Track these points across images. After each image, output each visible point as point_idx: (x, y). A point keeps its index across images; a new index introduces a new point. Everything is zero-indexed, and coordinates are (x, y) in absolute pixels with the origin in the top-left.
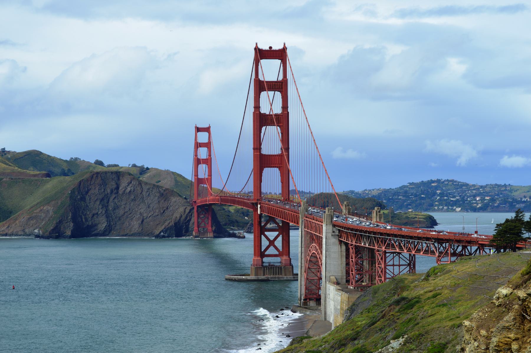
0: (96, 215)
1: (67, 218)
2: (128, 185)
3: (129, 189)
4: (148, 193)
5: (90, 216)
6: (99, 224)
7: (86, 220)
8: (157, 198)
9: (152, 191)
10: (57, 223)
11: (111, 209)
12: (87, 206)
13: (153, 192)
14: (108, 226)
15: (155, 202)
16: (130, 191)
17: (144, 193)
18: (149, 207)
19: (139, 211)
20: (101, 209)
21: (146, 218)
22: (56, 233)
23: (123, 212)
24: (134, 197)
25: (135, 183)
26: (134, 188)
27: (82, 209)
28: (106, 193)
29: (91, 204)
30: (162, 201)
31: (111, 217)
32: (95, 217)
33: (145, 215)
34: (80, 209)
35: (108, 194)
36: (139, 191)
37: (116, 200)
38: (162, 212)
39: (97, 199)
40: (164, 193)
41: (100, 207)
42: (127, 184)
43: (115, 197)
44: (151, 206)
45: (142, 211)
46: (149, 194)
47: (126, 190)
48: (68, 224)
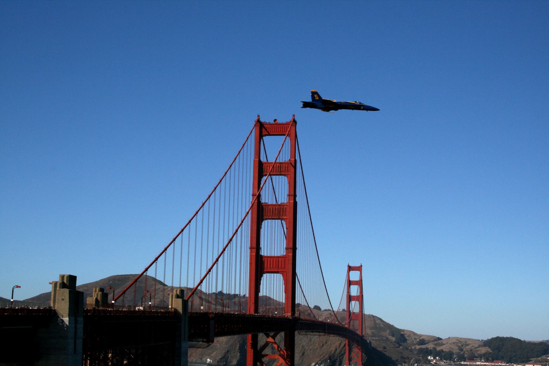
21: (308, 350)
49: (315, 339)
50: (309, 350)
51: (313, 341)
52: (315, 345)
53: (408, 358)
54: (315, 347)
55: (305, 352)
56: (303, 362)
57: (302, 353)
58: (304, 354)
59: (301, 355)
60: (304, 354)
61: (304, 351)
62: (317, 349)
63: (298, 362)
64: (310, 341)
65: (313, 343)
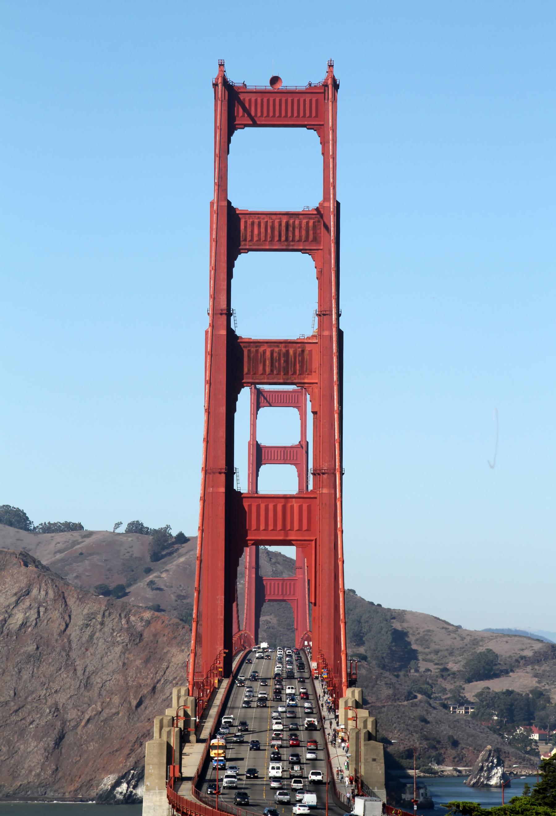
2: (17, 603)
3: (19, 617)
4: (88, 631)
8: (118, 649)
9: (102, 624)
13: (106, 629)
15: (113, 666)
16: (24, 625)
17: (74, 632)
21: (77, 726)
24: (38, 648)
25: (43, 593)
26: (39, 612)
30: (138, 662)
33: (72, 715)
36: (57, 626)
40: (145, 635)
42: (14, 599)
44: (97, 680)
45: (62, 698)
46: (91, 637)
47: (10, 621)
49: (104, 678)
50: (83, 723)
51: (100, 685)
52: (108, 703)
53: (455, 744)
54: (107, 711)
55: (66, 729)
56: (60, 774)
57: (54, 734)
58: (61, 738)
59: (52, 744)
60: (61, 738)
61: (63, 729)
62: (118, 713)
63: (38, 775)
64: (86, 686)
65: (100, 694)
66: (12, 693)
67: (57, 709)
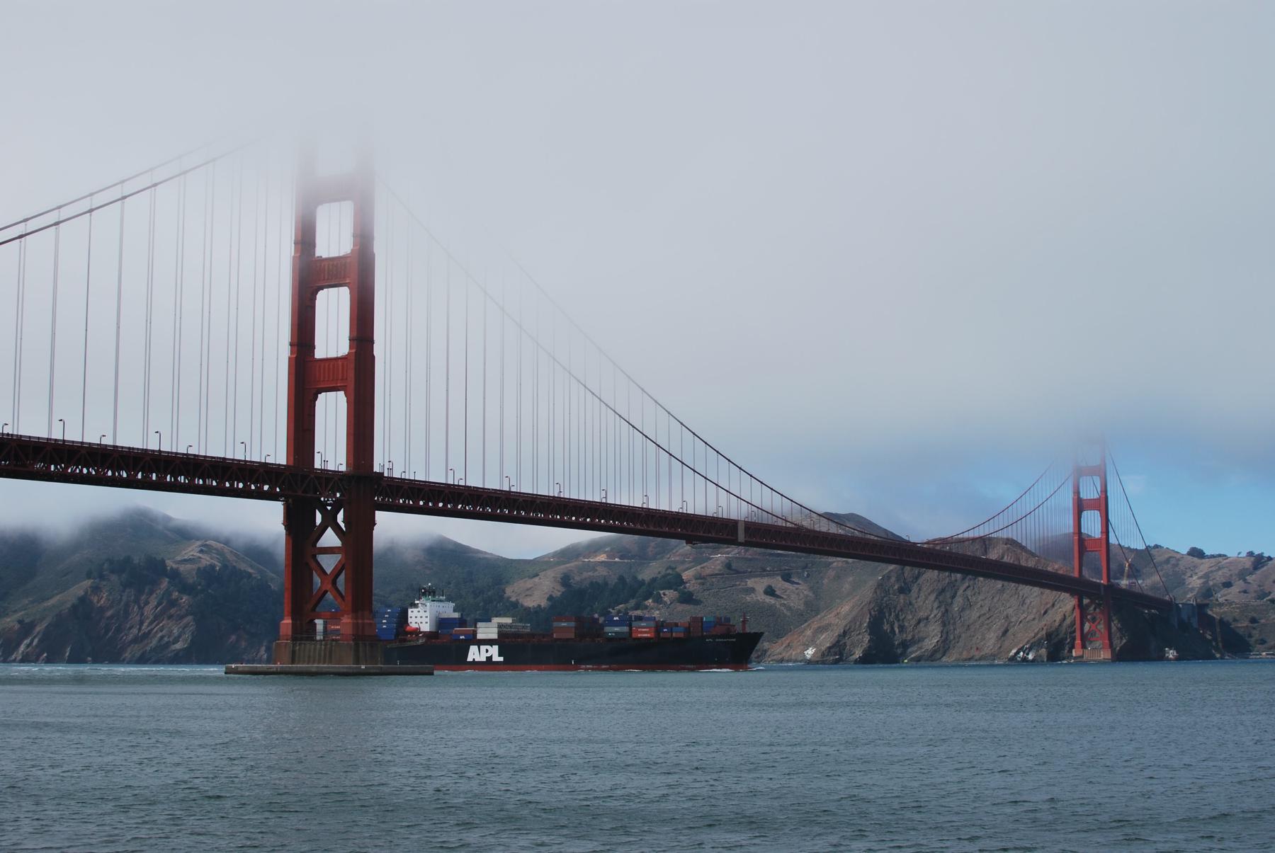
0: (925, 621)
1: (861, 624)
5: (913, 622)
6: (926, 638)
7: (902, 628)
10: (839, 636)
11: (956, 609)
12: (911, 604)
14: (942, 642)
18: (1023, 603)
19: (1005, 613)
20: (937, 609)
22: (836, 654)
23: (978, 614)
27: (898, 608)
28: (953, 579)
29: (919, 600)
31: (954, 623)
32: (922, 625)
34: (893, 610)
35: (956, 581)
37: (969, 593)
38: (1042, 612)
39: (932, 592)
41: (936, 605)
43: (969, 586)
44: (1028, 601)
45: (1010, 611)
48: (860, 637)
57: (1003, 630)
66: (987, 609)
67: (1007, 617)
